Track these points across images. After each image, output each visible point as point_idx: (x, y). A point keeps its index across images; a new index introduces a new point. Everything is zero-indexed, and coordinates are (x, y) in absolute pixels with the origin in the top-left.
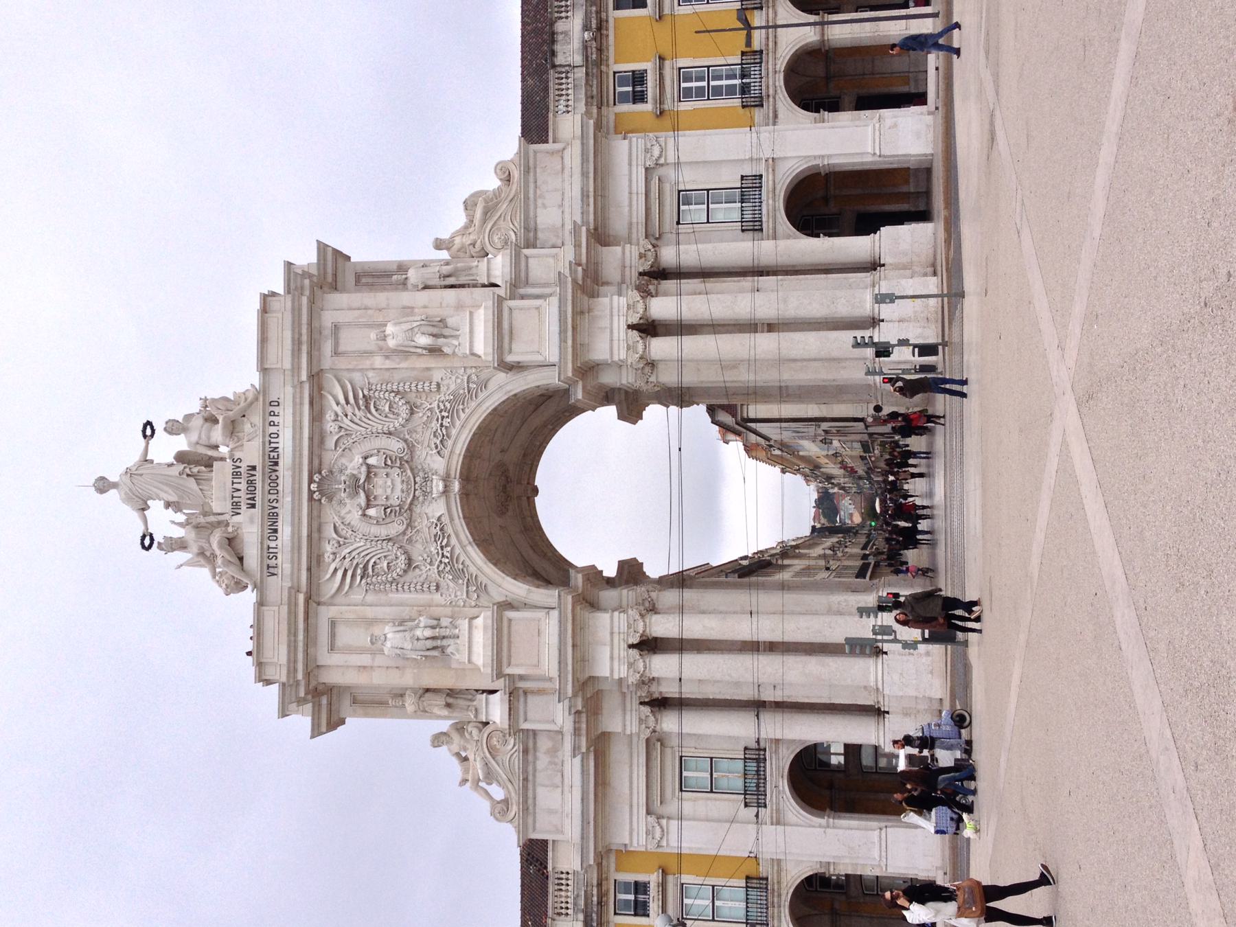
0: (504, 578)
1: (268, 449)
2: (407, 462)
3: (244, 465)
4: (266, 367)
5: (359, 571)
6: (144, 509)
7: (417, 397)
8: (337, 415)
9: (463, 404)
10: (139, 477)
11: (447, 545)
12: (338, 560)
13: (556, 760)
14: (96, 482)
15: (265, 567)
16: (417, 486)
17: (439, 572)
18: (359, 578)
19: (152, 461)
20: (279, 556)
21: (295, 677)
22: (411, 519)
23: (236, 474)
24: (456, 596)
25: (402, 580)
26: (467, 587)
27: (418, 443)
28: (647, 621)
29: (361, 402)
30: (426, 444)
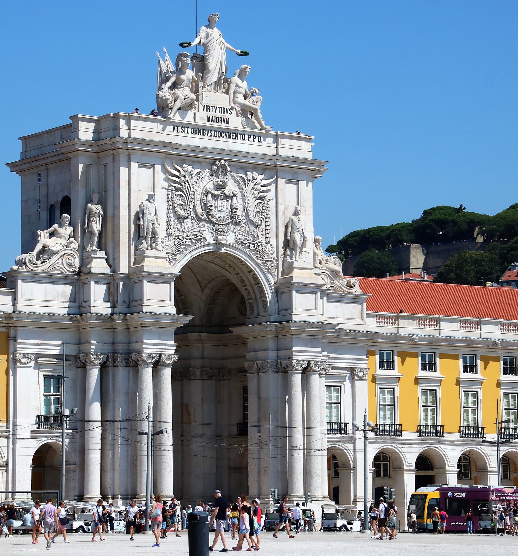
1: (237, 132)
9: (260, 257)
11: (192, 242)
12: (184, 173)
13: (60, 297)
15: (178, 125)
17: (178, 236)
20: (183, 134)
23: (224, 110)
24: (165, 245)
26: (171, 253)
29: (262, 194)
30: (241, 233)
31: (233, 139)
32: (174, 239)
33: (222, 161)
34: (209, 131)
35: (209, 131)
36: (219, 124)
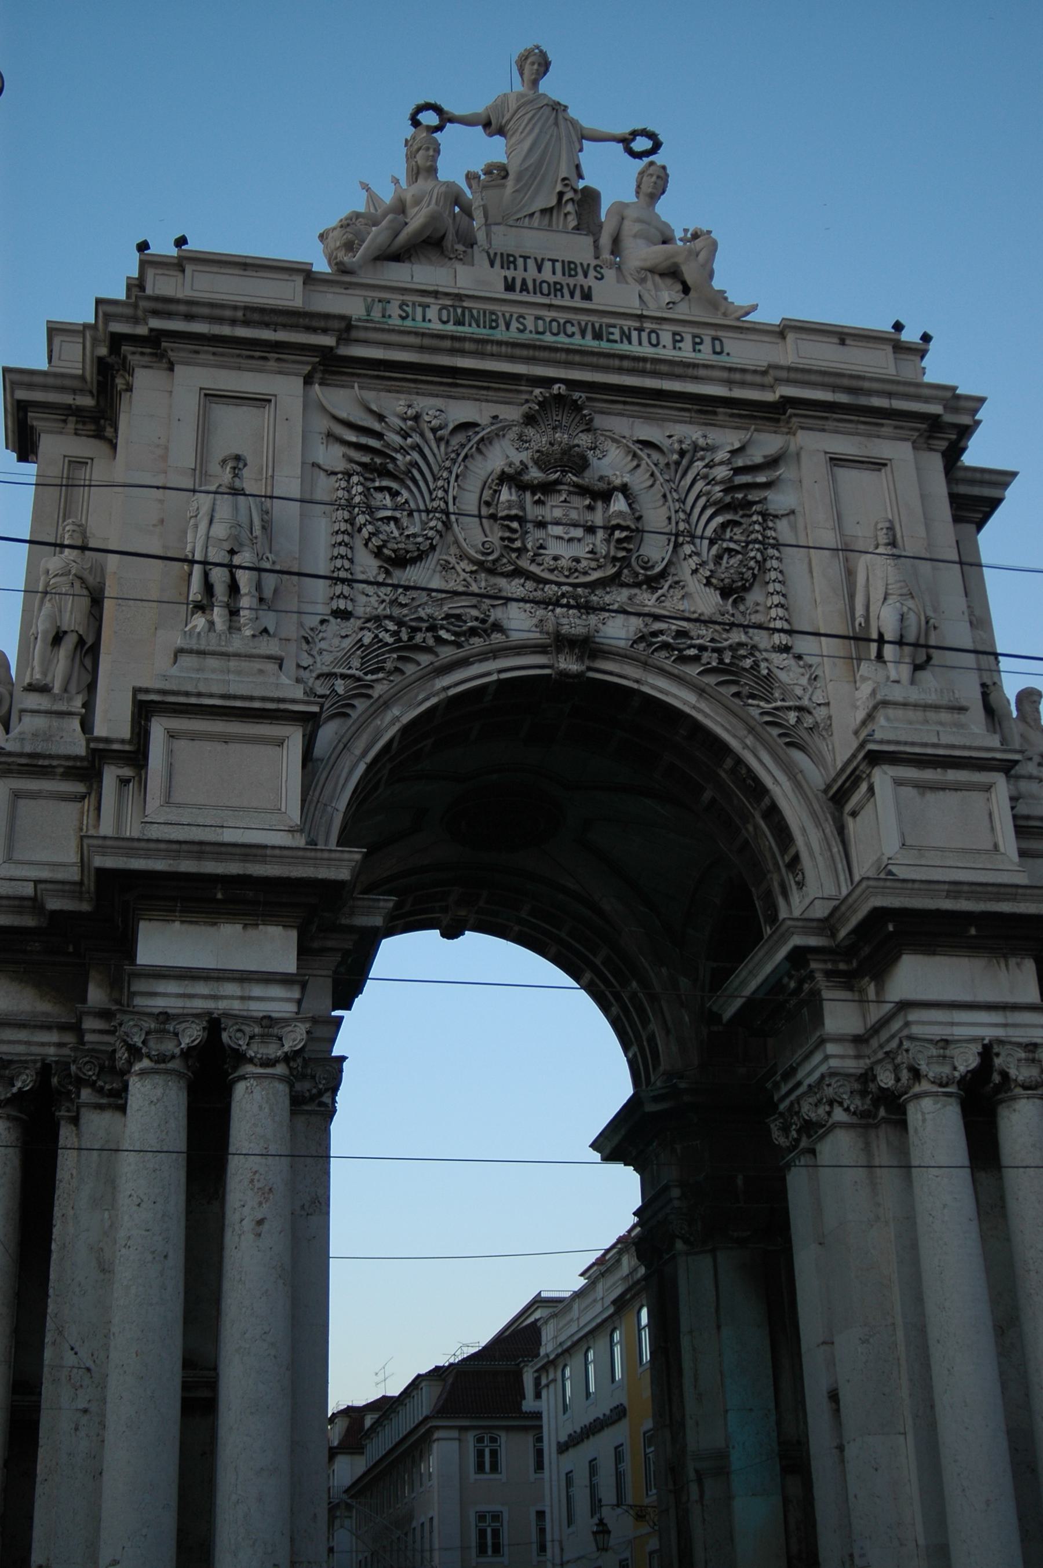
0: (364, 754)
2: (618, 574)
3: (591, 281)
4: (791, 337)
5: (378, 461)
6: (490, 125)
7: (758, 604)
8: (710, 448)
9: (753, 696)
10: (551, 120)
14: (541, 51)
16: (570, 589)
17: (377, 619)
18: (366, 459)
19: (581, 150)
21: (156, 313)
22: (492, 572)
23: (570, 268)
25: (358, 543)
26: (344, 676)
27: (658, 599)
28: (280, 1069)
29: (740, 496)
31: (609, 341)
32: (362, 629)
33: (556, 386)
34: (515, 316)
35: (515, 316)
36: (552, 296)
